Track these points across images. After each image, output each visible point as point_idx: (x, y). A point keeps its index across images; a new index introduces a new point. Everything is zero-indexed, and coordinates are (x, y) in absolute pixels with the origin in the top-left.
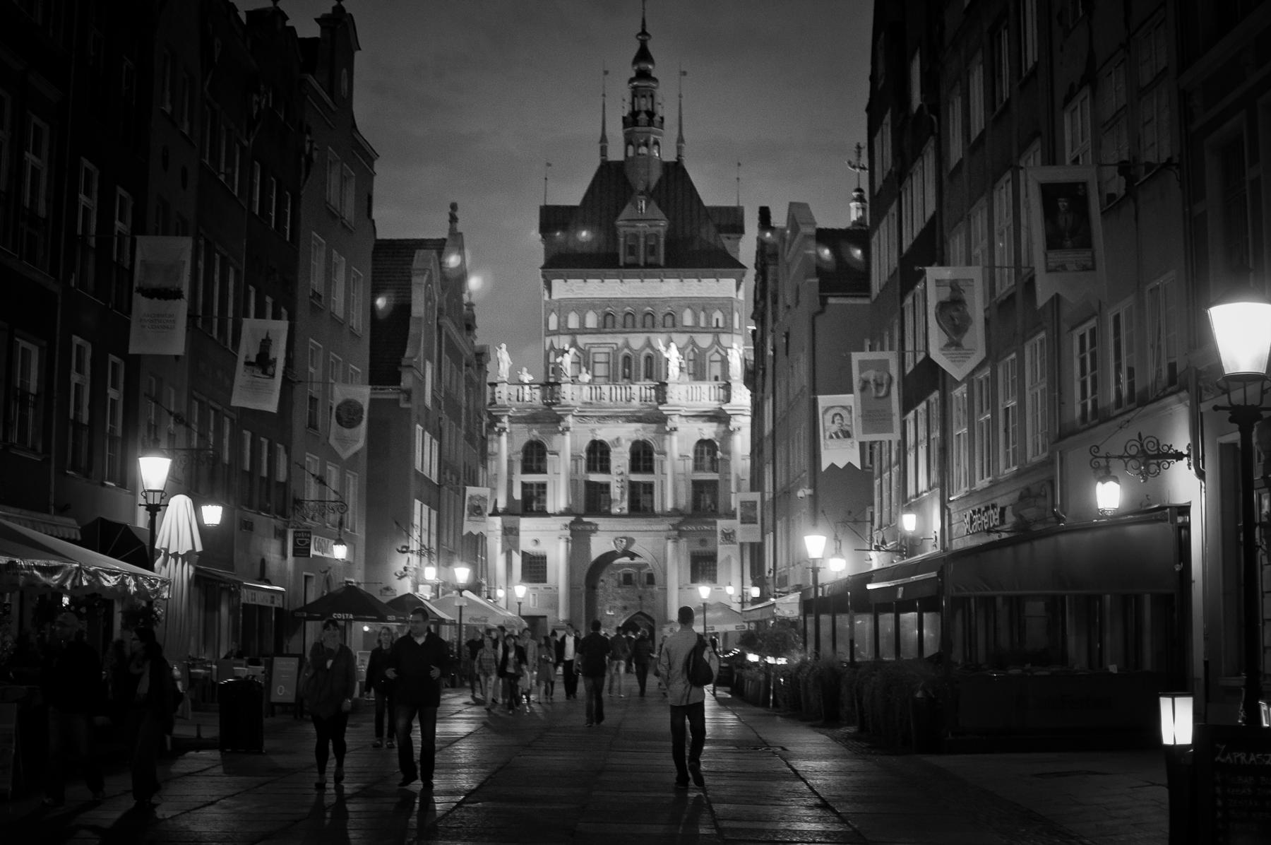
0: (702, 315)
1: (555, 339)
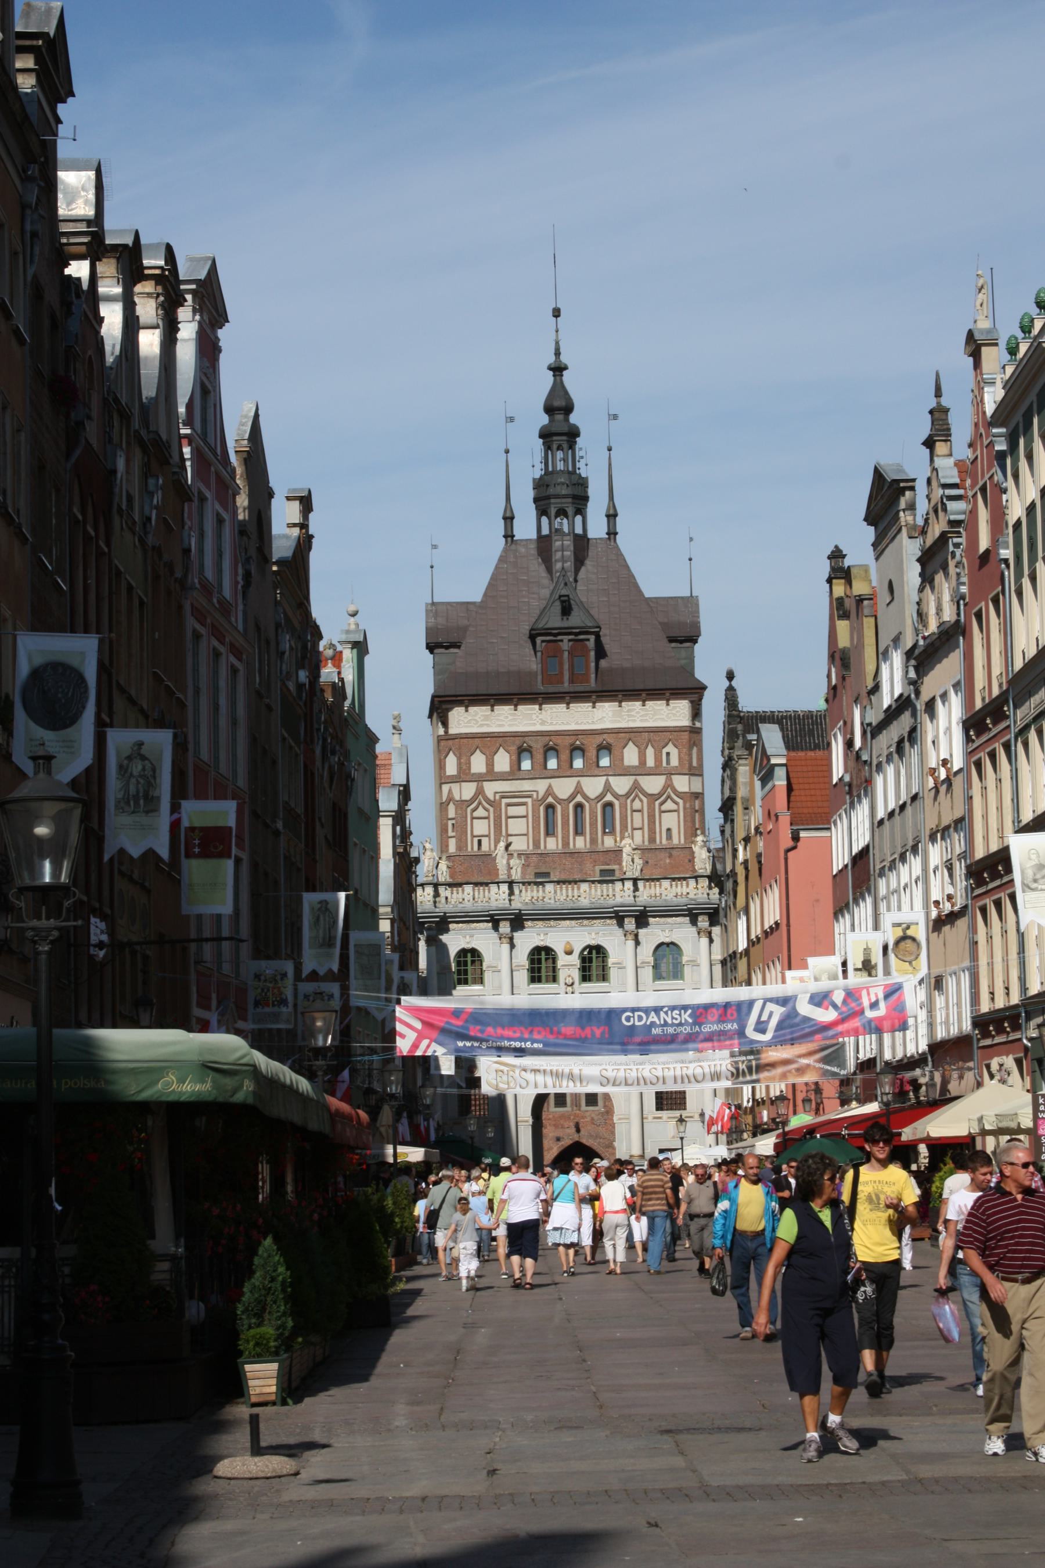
0: (650, 752)
1: (455, 787)
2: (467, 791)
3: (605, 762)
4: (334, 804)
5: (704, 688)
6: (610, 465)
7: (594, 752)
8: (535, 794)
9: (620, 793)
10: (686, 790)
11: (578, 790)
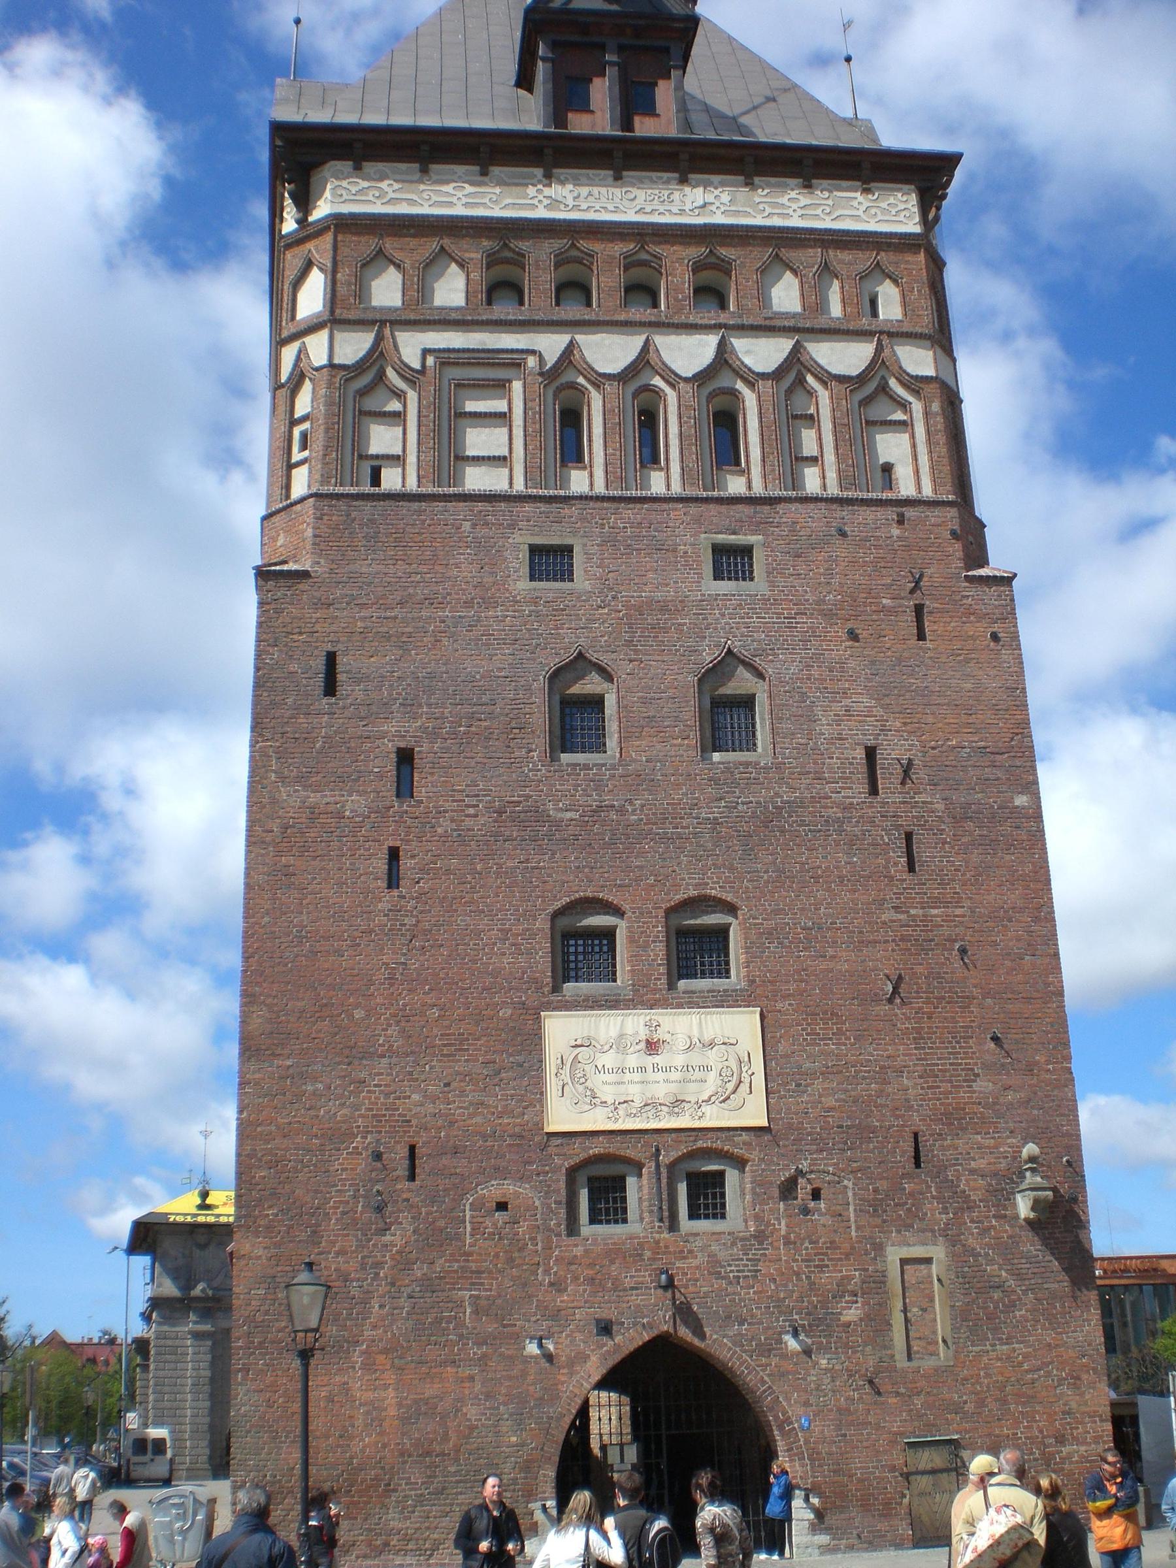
8: (532, 361)
9: (759, 369)
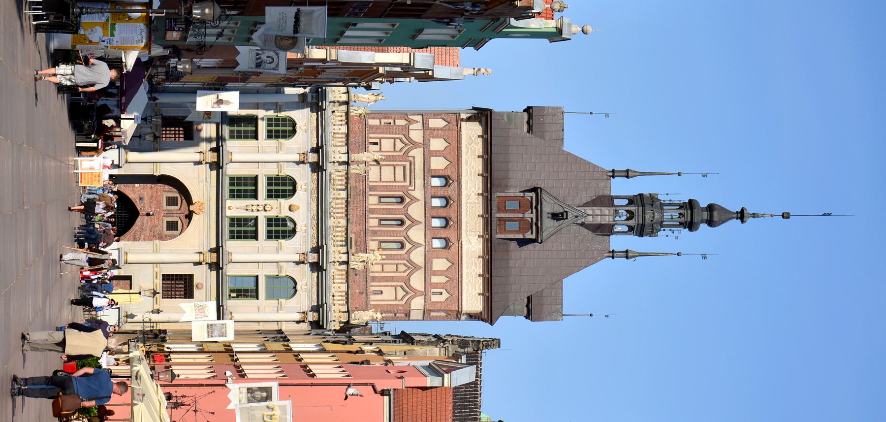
0: (442, 279)
1: (419, 126)
2: (416, 135)
3: (437, 244)
4: (430, 5)
5: (492, 324)
6: (667, 254)
7: (444, 236)
8: (412, 188)
10: (412, 307)
11: (414, 222)
